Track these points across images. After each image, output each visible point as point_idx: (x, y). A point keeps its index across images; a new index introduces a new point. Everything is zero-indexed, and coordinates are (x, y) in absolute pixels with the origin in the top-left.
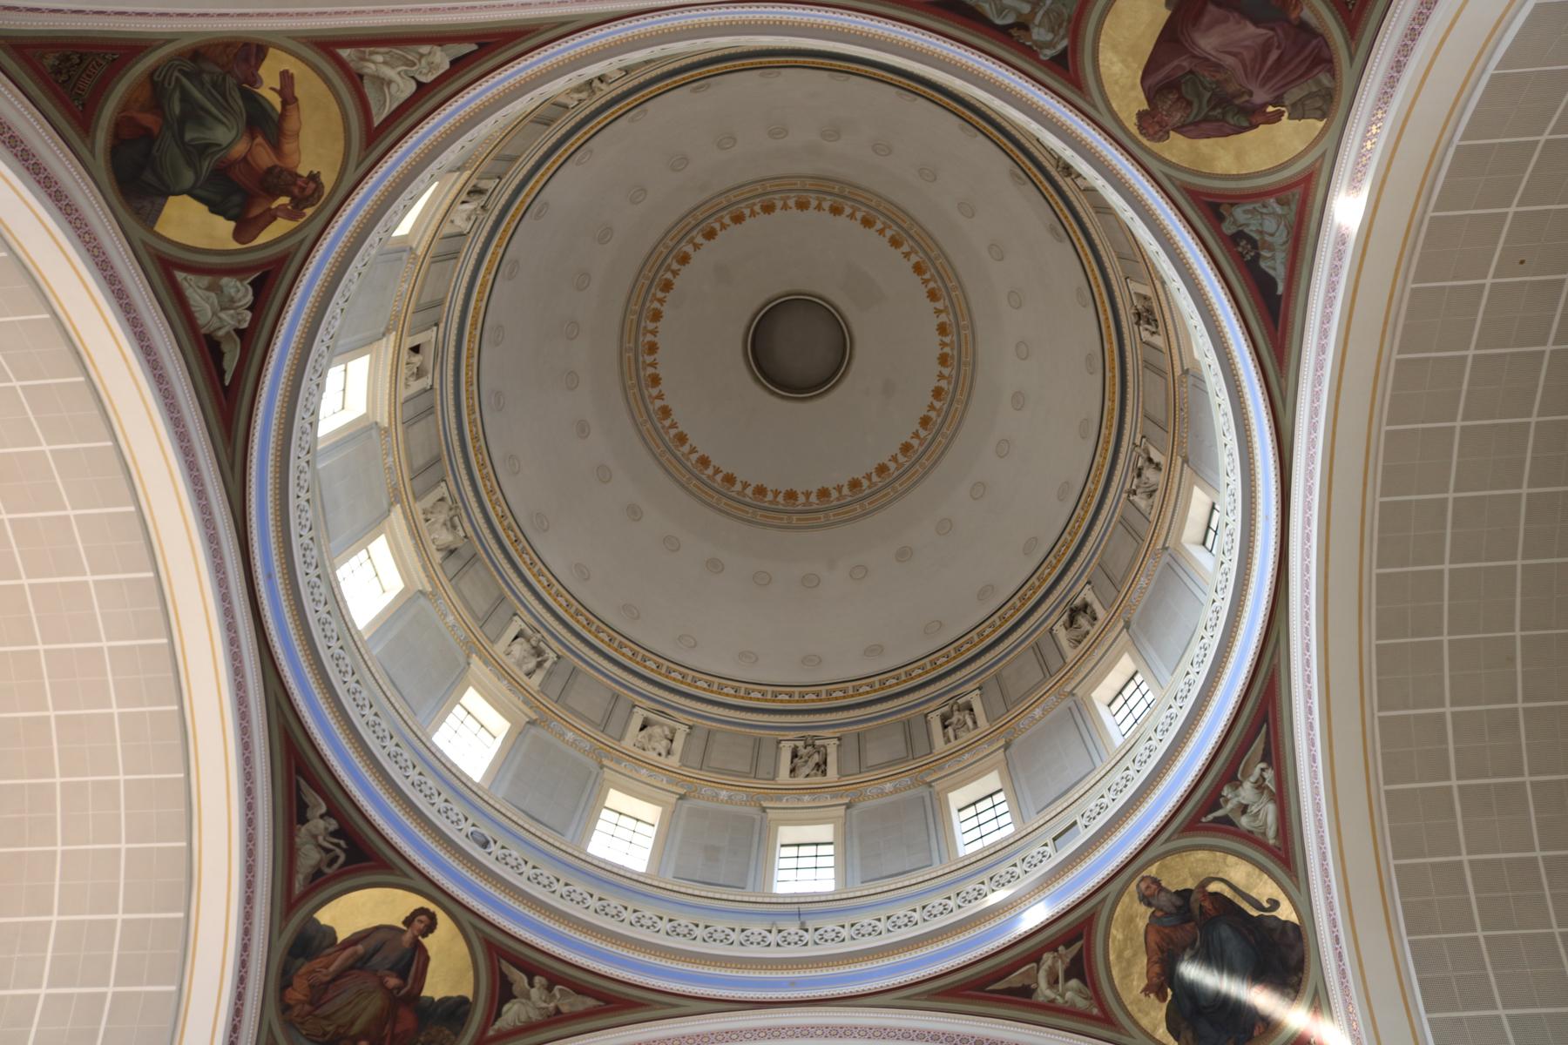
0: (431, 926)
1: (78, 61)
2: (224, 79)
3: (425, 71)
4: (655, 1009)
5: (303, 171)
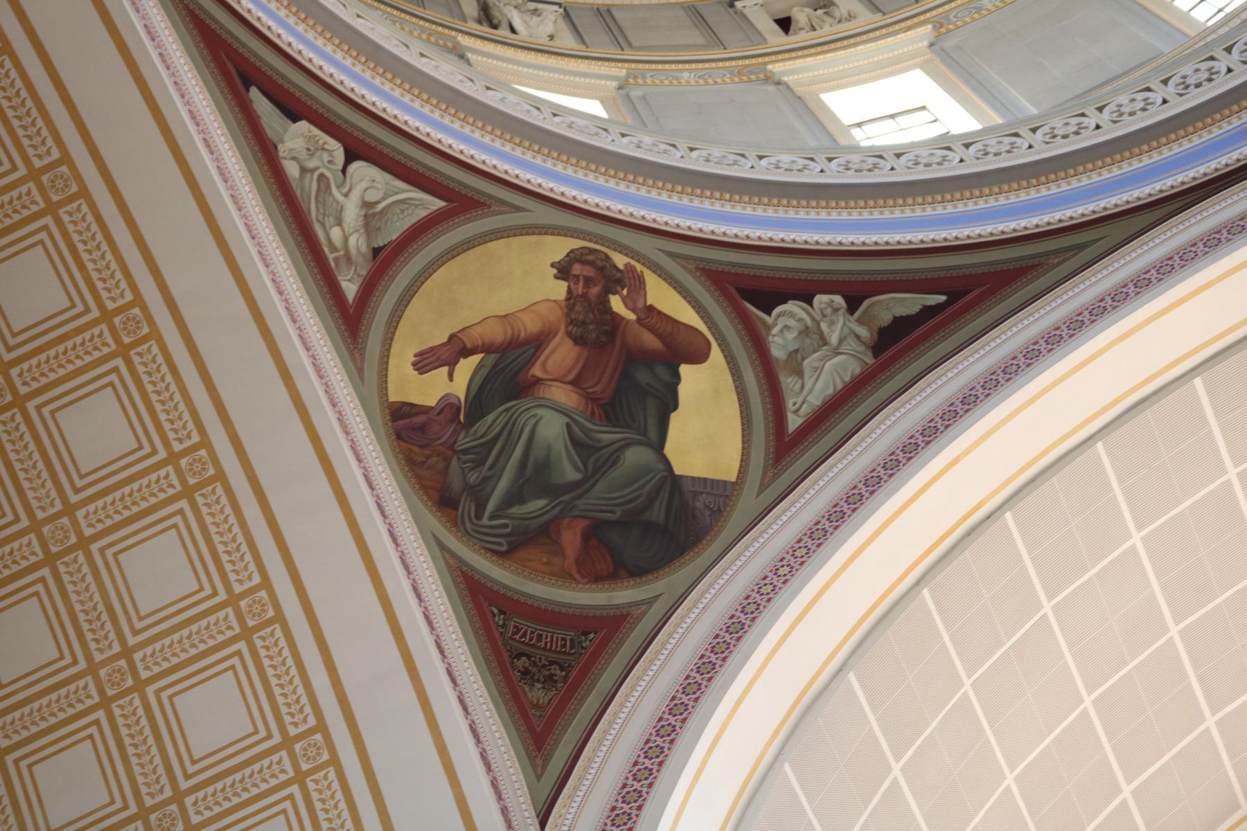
1: (524, 658)
3: (326, 157)
5: (559, 290)
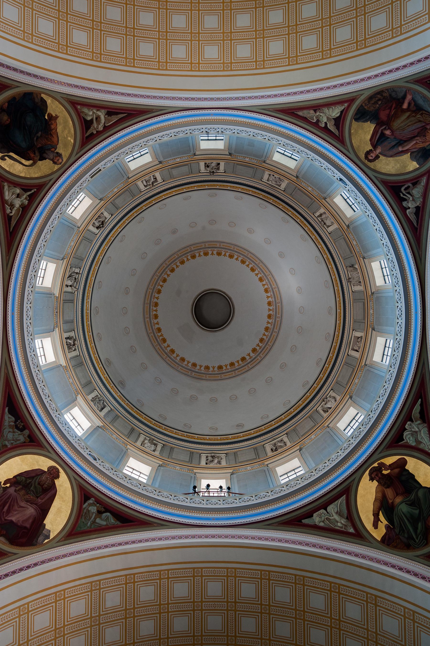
0: (368, 153)
3: (323, 515)
4: (272, 108)
5: (375, 483)
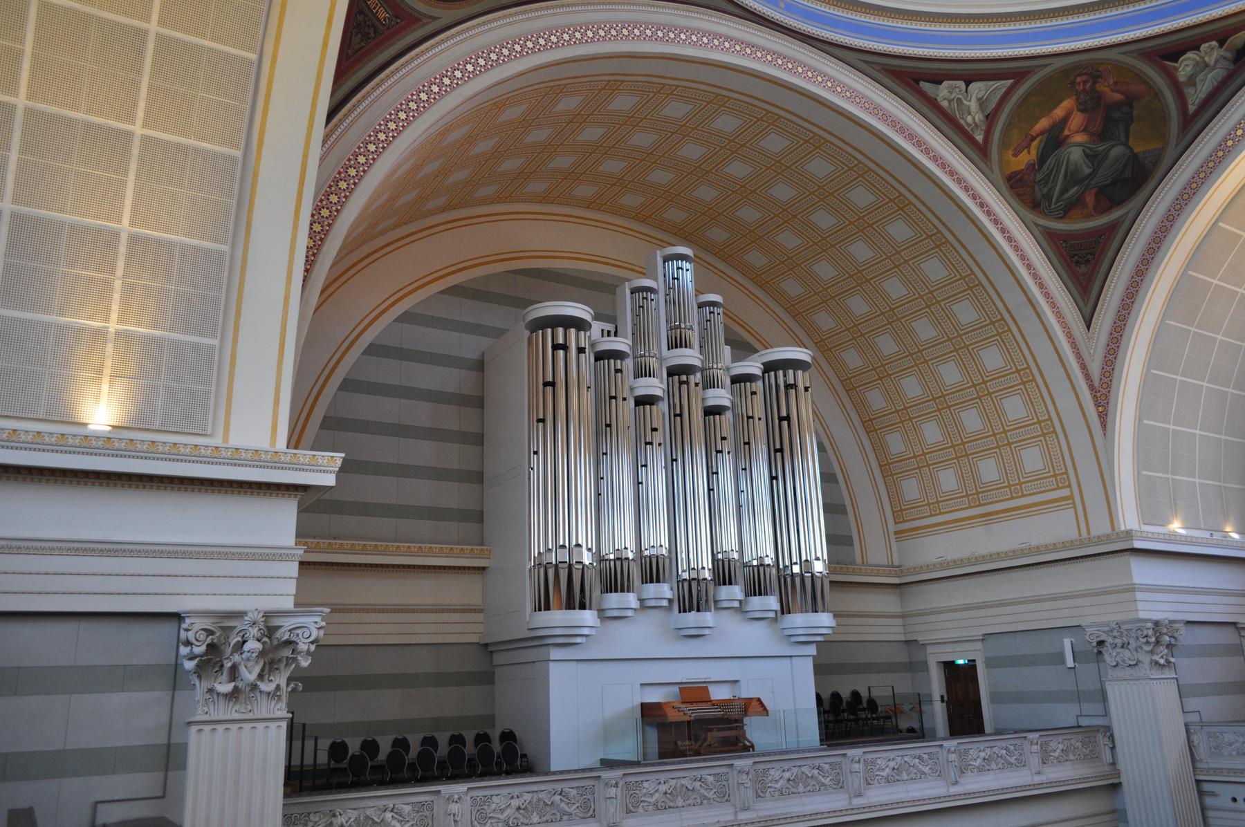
2: (1041, 180)
3: (957, 90)
